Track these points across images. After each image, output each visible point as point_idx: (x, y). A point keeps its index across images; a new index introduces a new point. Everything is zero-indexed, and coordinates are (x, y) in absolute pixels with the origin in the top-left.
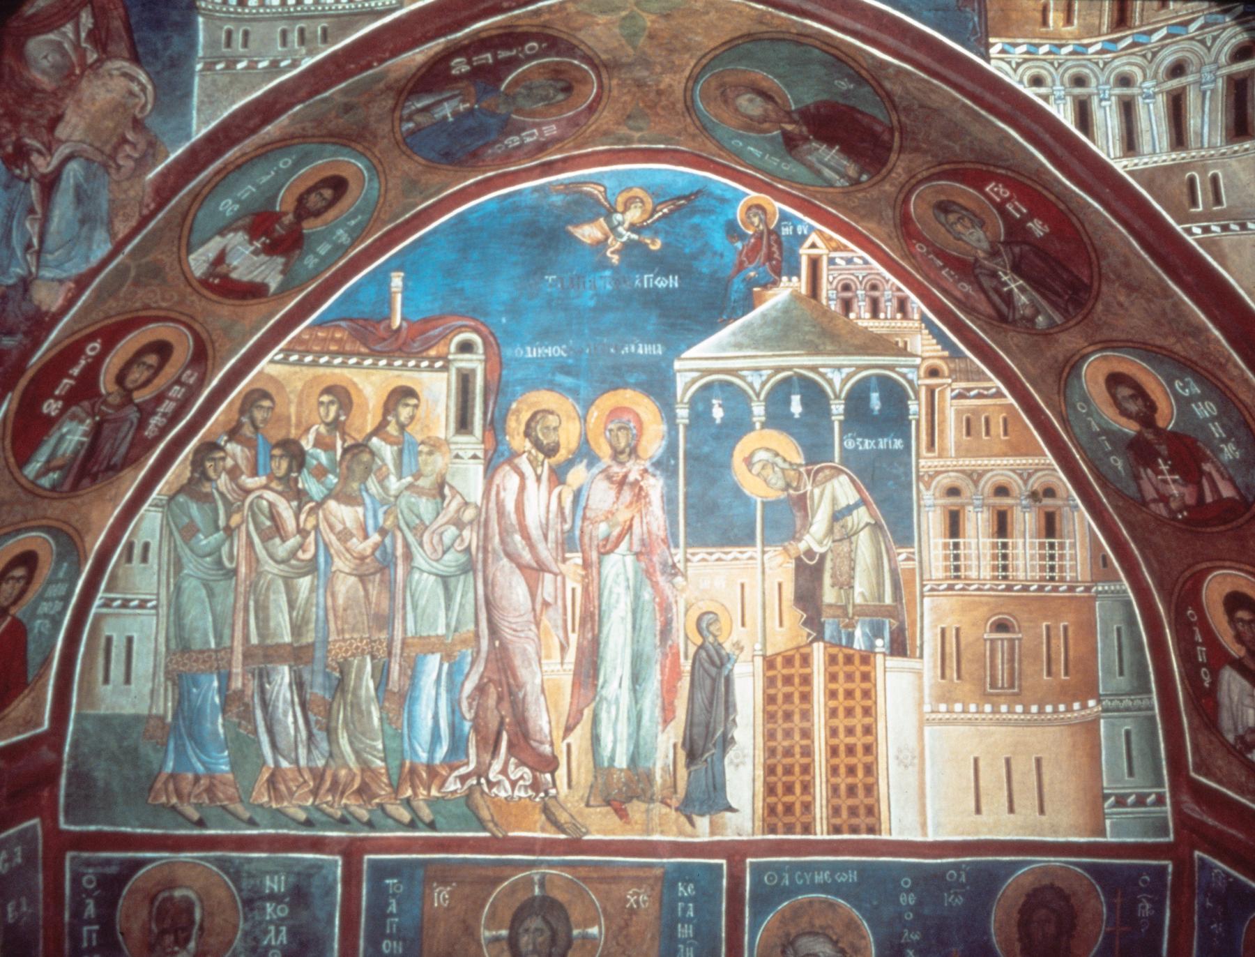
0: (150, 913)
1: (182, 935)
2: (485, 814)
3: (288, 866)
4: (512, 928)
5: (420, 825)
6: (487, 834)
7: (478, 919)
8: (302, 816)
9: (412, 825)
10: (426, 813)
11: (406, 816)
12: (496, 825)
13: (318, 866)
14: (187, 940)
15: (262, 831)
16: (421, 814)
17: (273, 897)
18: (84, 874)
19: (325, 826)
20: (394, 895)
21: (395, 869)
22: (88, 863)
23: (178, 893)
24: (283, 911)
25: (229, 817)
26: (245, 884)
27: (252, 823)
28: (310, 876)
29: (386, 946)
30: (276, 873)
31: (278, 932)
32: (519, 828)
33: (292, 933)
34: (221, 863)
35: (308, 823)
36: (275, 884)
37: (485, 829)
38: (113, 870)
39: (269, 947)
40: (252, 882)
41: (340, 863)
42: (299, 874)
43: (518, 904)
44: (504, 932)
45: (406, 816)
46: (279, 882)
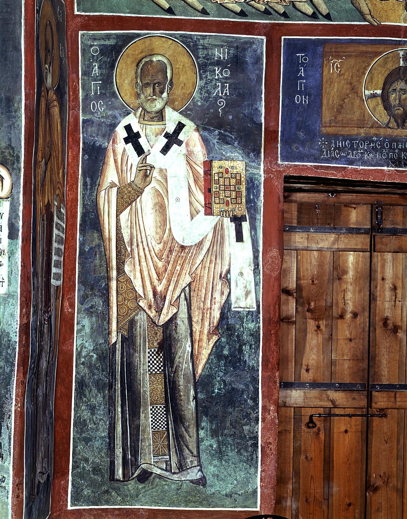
0: (136, 73)
1: (157, 89)
2: (365, 10)
3: (230, 44)
4: (383, 89)
5: (320, 16)
6: (367, 23)
7: (360, 83)
8: (238, 9)
9: (314, 16)
10: (324, 9)
11: (310, 10)
12: (373, 17)
13: (251, 43)
14: (162, 92)
15: (211, 18)
16: (320, 10)
17: (219, 63)
18: (91, 46)
19: (254, 16)
20: (302, 64)
21: (303, 46)
22: (94, 38)
23: (155, 59)
24: (227, 74)
25: (189, 8)
26: (201, 53)
27: (204, 12)
28: (244, 50)
29: (298, 99)
30: (222, 46)
31: (223, 87)
32: (388, 20)
33: (233, 87)
34: (184, 39)
35: (242, 14)
36: (218, 54)
37: (365, 20)
38: (112, 42)
39: (217, 97)
40: (206, 52)
41: (265, 41)
42: (237, 48)
43: (388, 72)
44: (379, 92)
45: (310, 10)
46: (224, 53)
